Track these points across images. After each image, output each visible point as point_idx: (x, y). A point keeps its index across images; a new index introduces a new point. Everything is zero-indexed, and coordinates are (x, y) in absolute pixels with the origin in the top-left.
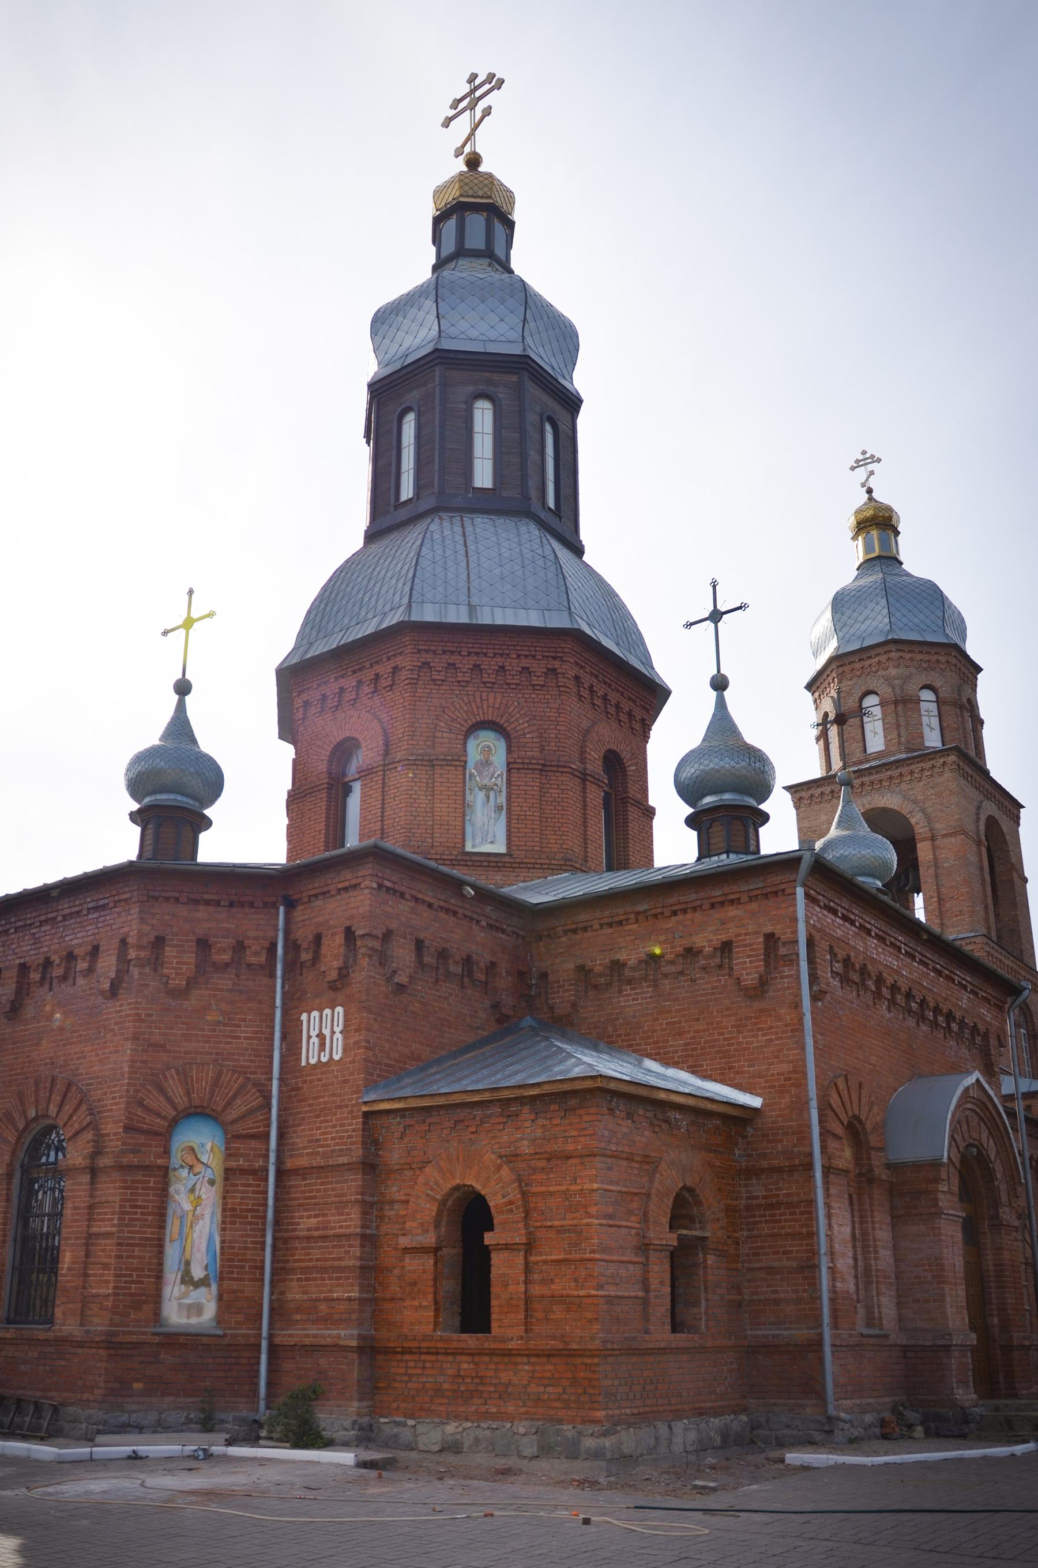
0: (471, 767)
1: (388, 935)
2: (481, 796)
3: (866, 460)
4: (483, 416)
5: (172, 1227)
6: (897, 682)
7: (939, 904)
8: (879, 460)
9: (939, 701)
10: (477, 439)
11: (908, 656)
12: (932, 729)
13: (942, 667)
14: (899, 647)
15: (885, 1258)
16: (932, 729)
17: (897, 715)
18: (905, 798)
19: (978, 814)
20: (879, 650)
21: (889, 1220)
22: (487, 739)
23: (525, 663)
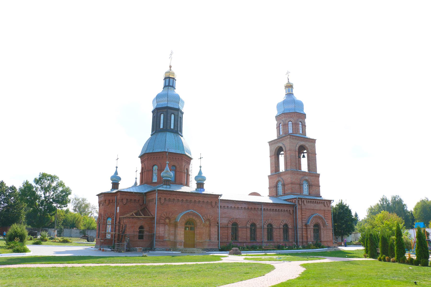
0: (154, 171)
1: (122, 199)
2: (155, 174)
3: (288, 73)
4: (162, 116)
5: (107, 228)
6: (284, 121)
7: (286, 164)
10: (161, 120)
11: (286, 116)
12: (291, 129)
13: (293, 117)
14: (285, 114)
15: (173, 232)
16: (291, 129)
17: (284, 128)
19: (297, 145)
20: (282, 115)
21: (174, 228)
23: (160, 156)
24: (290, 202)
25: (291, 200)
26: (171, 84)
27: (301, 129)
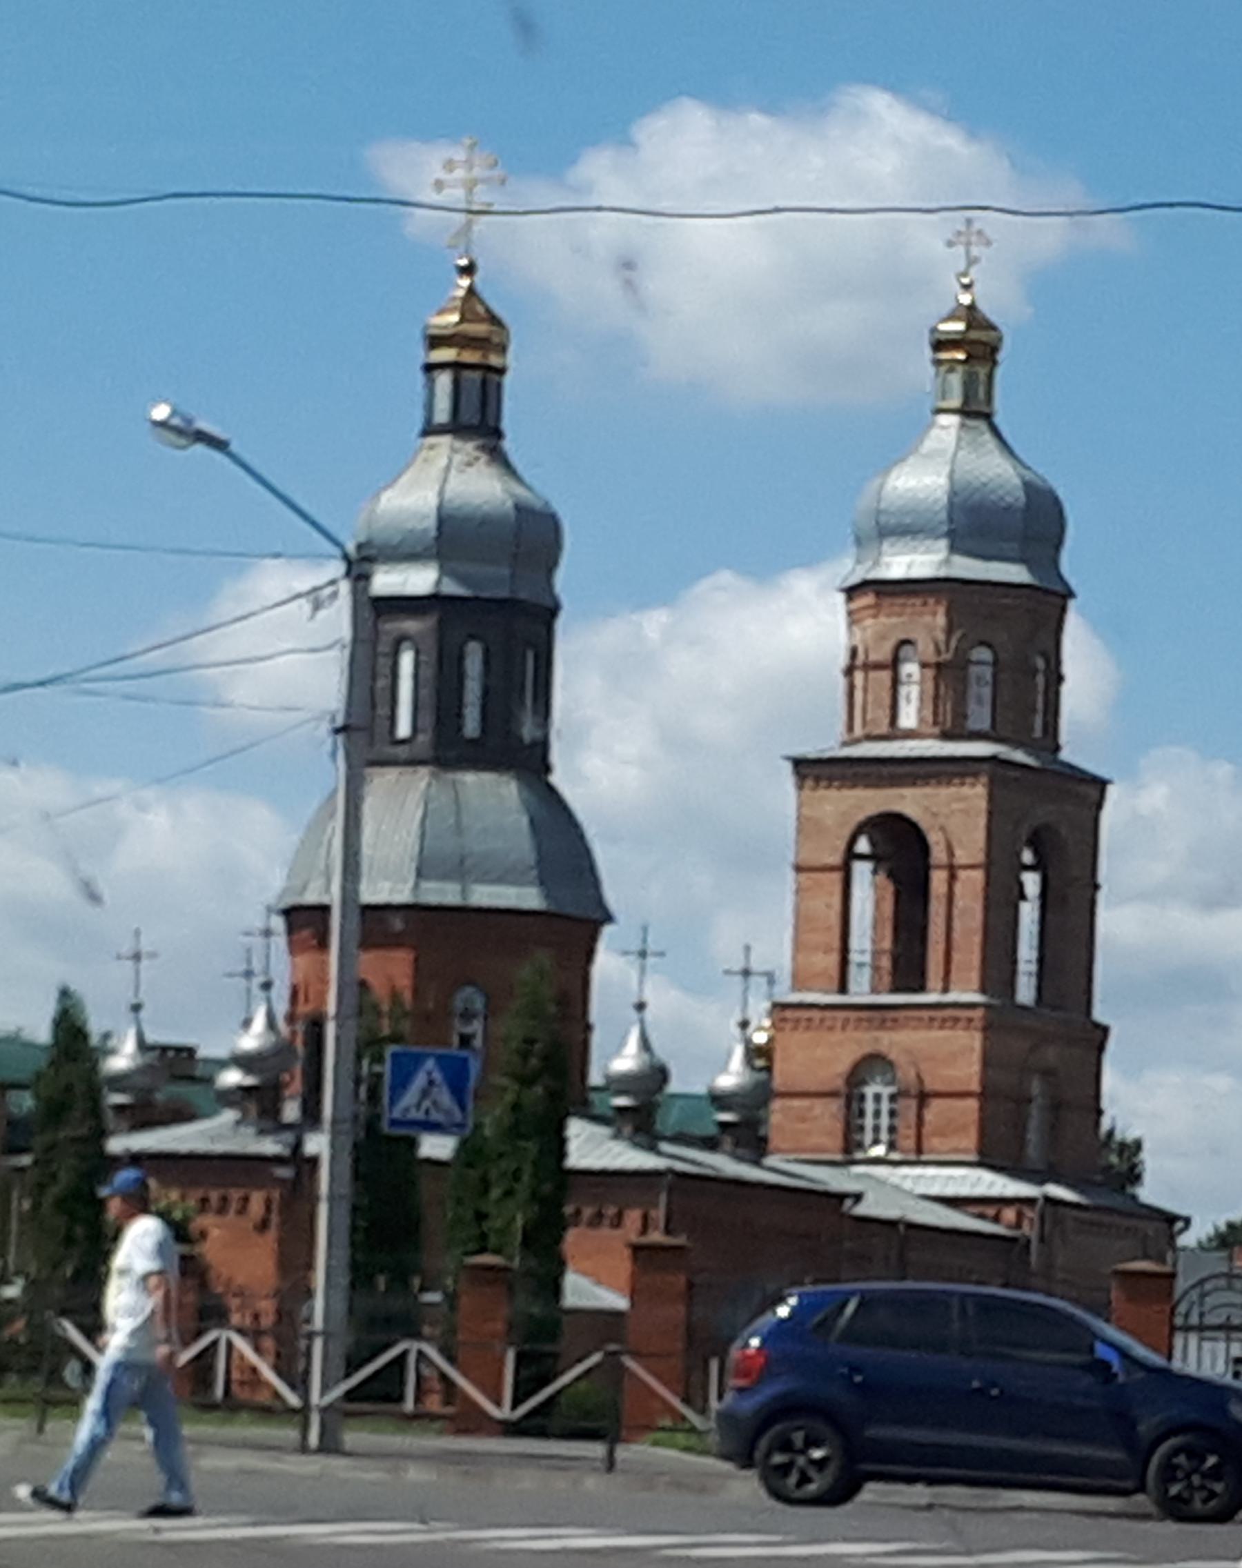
8: (988, 243)
9: (995, 663)
18: (927, 809)
22: (469, 990)
24: (981, 1216)
25: (991, 1211)
26: (491, 423)
27: (1040, 705)
